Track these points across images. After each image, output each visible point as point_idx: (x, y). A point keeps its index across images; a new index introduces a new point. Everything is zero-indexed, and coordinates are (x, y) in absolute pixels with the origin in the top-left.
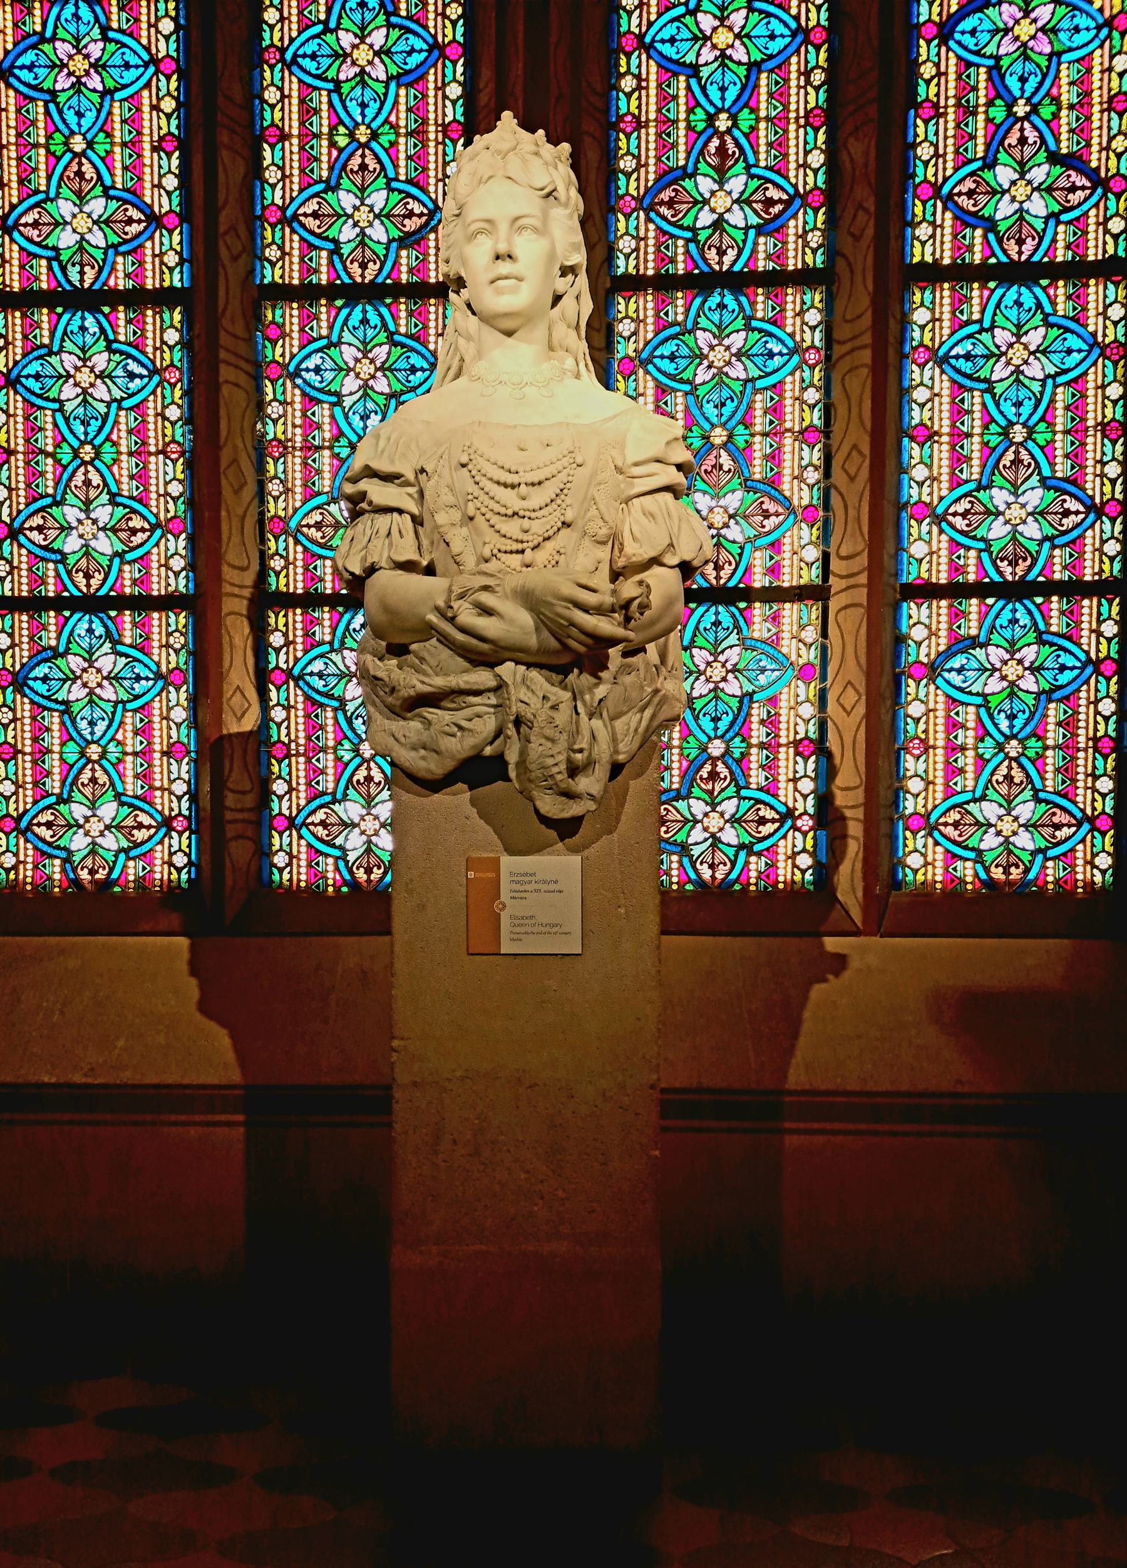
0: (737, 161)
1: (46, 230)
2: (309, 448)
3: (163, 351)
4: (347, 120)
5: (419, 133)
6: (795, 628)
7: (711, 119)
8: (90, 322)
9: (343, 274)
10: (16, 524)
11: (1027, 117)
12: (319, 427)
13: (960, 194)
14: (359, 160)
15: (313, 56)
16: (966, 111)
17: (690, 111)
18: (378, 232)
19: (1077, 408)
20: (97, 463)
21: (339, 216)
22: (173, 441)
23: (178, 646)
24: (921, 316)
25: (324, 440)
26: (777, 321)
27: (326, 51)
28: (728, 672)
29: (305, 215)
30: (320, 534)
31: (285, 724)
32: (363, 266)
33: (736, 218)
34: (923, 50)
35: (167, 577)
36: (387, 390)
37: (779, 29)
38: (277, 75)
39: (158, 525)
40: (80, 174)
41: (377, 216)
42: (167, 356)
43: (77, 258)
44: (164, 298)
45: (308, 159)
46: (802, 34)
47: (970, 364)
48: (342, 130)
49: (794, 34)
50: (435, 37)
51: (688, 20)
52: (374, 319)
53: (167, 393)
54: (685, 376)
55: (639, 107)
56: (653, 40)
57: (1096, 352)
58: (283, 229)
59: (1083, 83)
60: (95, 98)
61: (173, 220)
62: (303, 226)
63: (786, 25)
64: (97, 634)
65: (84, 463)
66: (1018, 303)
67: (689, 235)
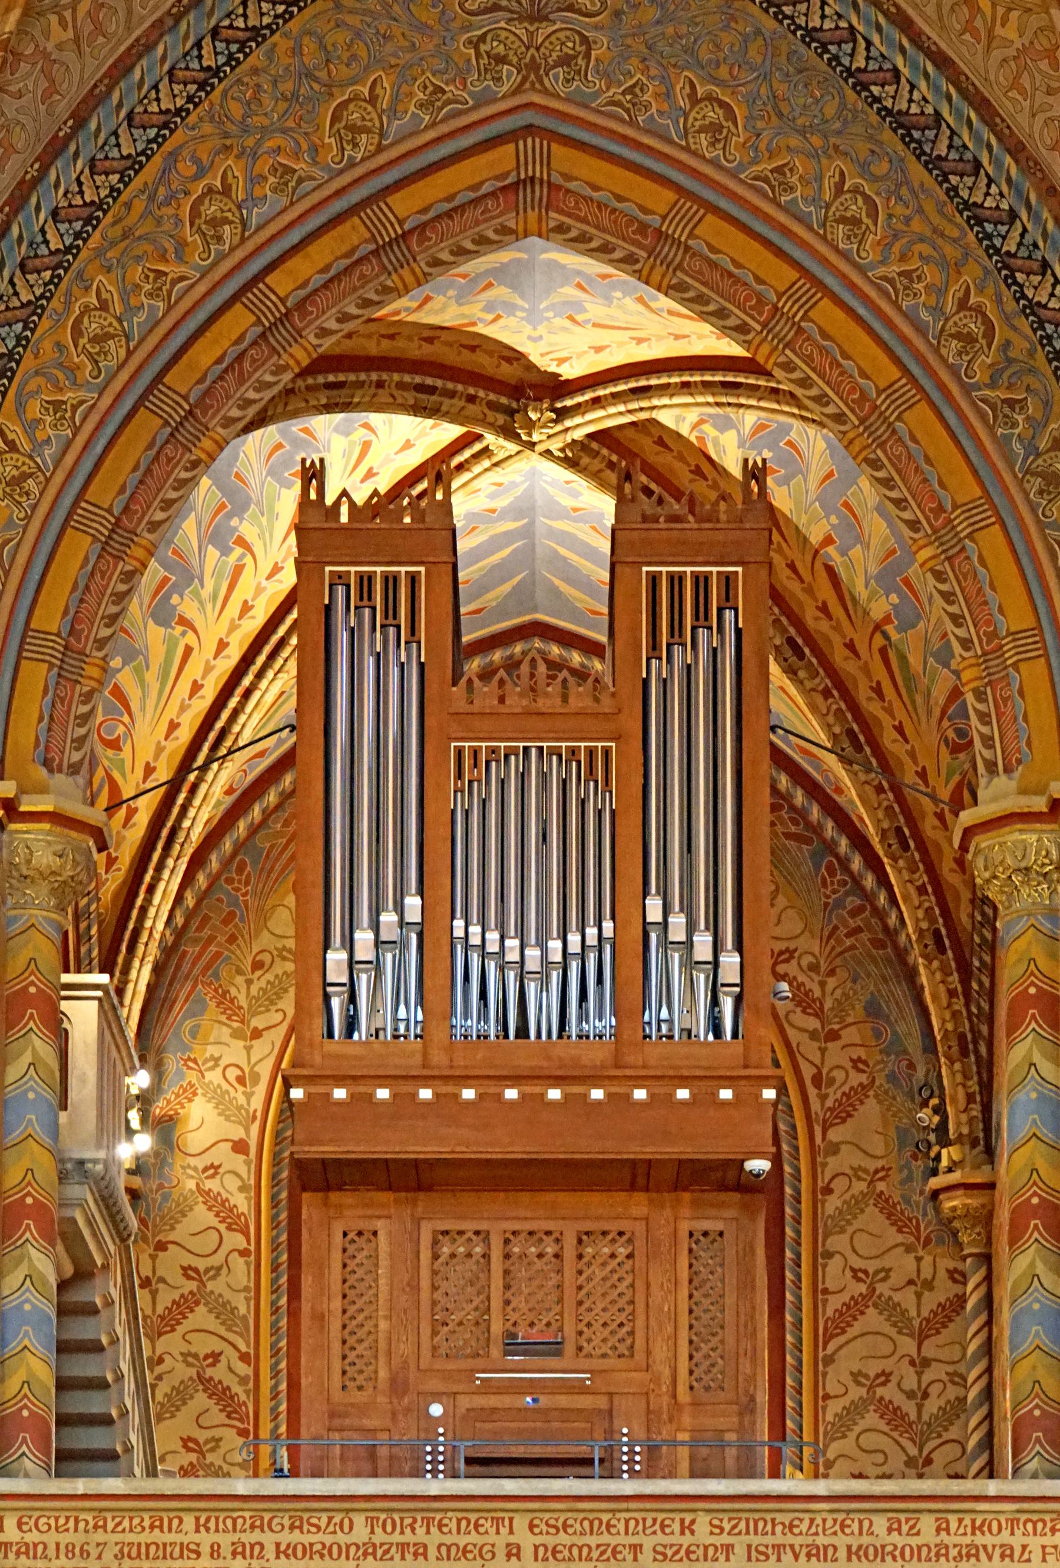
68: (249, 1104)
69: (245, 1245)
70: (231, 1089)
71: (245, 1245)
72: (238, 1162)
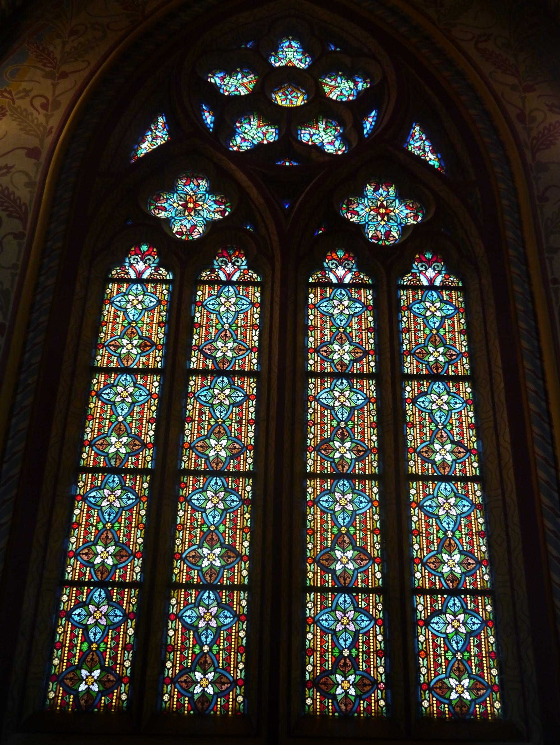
0: (348, 437)
1: (105, 446)
2: (192, 528)
3: (142, 490)
4: (215, 416)
5: (240, 422)
6: (374, 604)
7: (339, 423)
8: (116, 479)
9: (210, 467)
10: (78, 552)
11: (442, 429)
12: (197, 520)
13: (423, 452)
14: (218, 429)
15: (205, 396)
16: (423, 426)
17: (331, 421)
18: (223, 454)
19: (469, 526)
20: (112, 530)
21: (210, 447)
22: (142, 523)
23: (134, 603)
24: (413, 492)
25: (198, 525)
26: (364, 491)
27: (210, 394)
28: (349, 621)
29: (198, 446)
30: (193, 560)
31: (173, 637)
32: (217, 464)
33: (348, 455)
34: (407, 406)
35: (133, 575)
36: (223, 508)
37: (360, 397)
38: (192, 401)
39: (132, 554)
40: (120, 429)
41: (223, 448)
42: (143, 492)
43: (115, 457)
44: (144, 472)
46: (368, 400)
47: (431, 509)
48: (213, 419)
49: (365, 399)
50: (246, 392)
51: (330, 392)
52: (219, 482)
53: (142, 505)
54: (331, 508)
55: (314, 418)
56: (319, 398)
57: (473, 507)
58: (189, 451)
59: (460, 419)
60: (129, 405)
61: (151, 445)
62: (197, 450)
63: (363, 396)
64: (102, 597)
65: (107, 530)
66: (445, 489)
67: (332, 460)
68: (47, 123)
69: (21, 229)
70: (35, 112)
71: (21, 229)
72: (29, 165)
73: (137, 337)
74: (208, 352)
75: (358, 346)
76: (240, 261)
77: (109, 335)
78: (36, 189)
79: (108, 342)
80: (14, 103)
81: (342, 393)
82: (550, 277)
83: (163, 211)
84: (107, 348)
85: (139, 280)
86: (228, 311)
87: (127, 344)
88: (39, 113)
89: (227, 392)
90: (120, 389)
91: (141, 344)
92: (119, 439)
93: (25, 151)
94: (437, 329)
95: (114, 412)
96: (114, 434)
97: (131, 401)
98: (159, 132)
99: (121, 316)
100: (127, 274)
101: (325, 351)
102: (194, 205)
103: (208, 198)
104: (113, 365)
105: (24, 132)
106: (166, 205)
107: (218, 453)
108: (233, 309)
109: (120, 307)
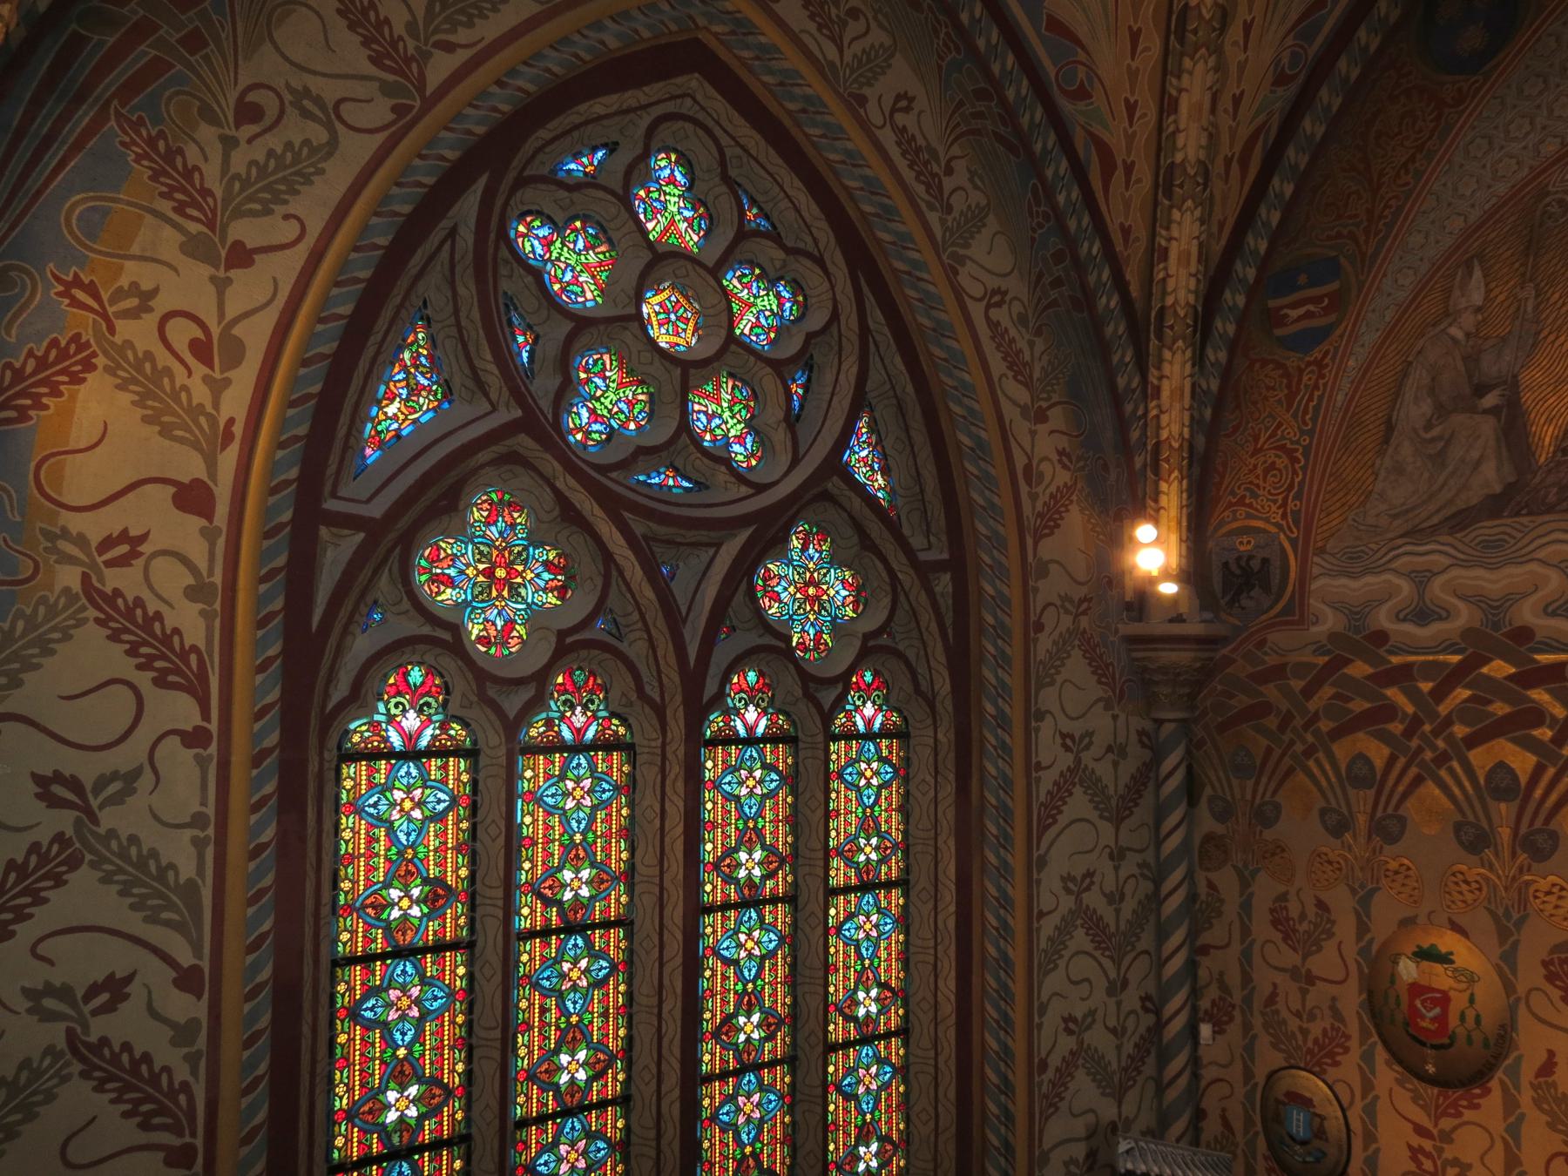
15: (548, 978)
27: (555, 974)
33: (756, 1035)
40: (402, 1072)
45: (544, 1038)
68: (216, 406)
69: (197, 720)
71: (197, 720)
72: (185, 532)
73: (419, 881)
74: (548, 893)
75: (770, 850)
76: (597, 701)
77: (362, 883)
78: (217, 606)
79: (361, 899)
80: (112, 329)
81: (749, 935)
82: (1034, 761)
83: (447, 586)
84: (361, 912)
85: (411, 754)
86: (579, 806)
87: (401, 899)
88: (190, 374)
89: (583, 964)
90: (394, 994)
91: (427, 896)
92: (402, 1093)
93: (172, 490)
94: (872, 807)
95: (387, 1041)
96: (392, 1085)
97: (417, 1014)
98: (423, 374)
99: (382, 838)
100: (386, 740)
101: (728, 866)
102: (508, 573)
103: (534, 557)
104: (378, 946)
105: (157, 428)
106: (452, 572)
107: (573, 1077)
108: (587, 802)
109: (379, 818)
